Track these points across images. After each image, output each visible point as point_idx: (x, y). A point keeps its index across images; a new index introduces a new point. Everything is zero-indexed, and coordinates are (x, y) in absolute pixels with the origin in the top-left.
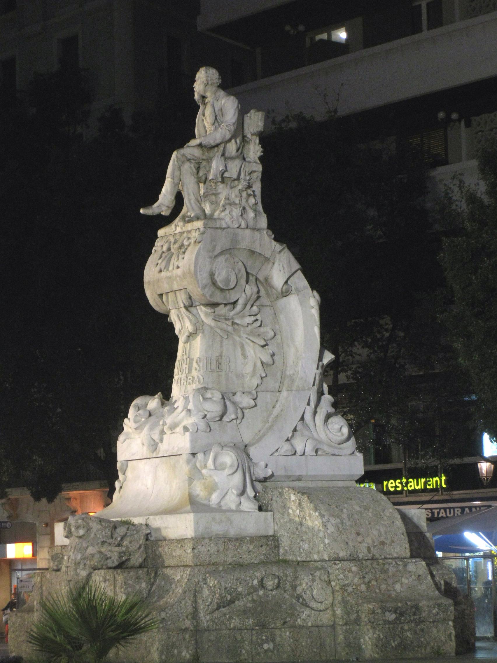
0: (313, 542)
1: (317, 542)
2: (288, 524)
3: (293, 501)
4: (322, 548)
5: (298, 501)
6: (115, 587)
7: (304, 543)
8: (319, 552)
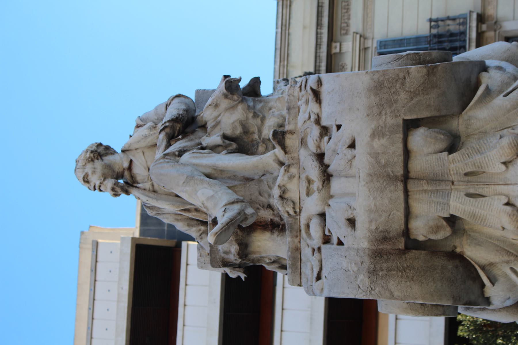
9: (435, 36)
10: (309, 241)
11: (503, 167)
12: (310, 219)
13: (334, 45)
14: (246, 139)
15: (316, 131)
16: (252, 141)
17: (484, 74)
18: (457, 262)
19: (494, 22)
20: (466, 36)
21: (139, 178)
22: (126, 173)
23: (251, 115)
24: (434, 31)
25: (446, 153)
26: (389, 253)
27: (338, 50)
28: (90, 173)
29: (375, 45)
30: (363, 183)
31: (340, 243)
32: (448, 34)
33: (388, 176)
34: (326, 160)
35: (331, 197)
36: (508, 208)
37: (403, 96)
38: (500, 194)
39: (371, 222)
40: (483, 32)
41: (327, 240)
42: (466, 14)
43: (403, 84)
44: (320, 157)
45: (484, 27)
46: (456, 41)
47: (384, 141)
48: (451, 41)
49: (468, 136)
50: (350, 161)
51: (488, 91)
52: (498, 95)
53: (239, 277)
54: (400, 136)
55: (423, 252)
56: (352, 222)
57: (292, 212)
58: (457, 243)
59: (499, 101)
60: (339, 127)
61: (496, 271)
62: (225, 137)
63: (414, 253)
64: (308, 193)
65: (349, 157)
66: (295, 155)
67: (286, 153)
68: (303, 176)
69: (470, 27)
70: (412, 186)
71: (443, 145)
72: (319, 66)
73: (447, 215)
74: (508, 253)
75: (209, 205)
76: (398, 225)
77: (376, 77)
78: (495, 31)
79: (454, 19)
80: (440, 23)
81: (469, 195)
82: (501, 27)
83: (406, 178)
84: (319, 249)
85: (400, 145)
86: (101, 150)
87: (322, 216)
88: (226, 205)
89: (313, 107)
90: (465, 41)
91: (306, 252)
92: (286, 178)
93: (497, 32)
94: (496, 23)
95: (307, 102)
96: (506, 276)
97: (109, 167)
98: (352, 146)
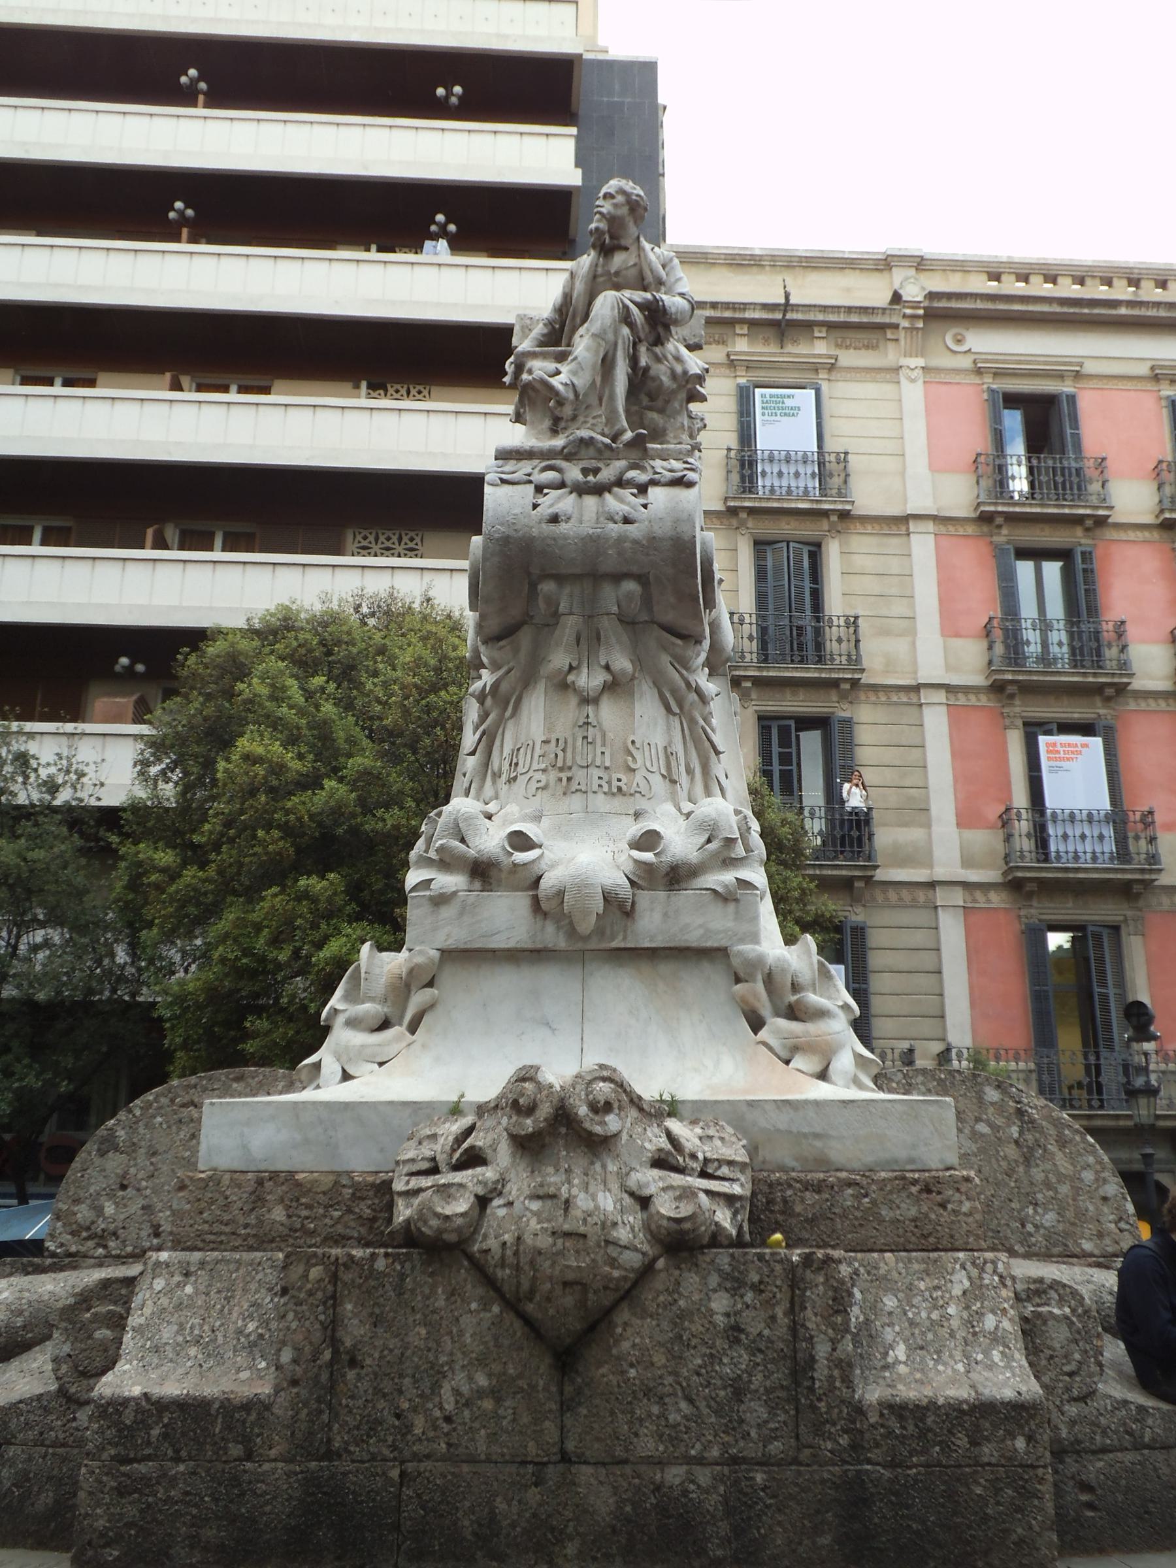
1: (1091, 1208)
3: (992, 1104)
6: (795, 1307)
11: (603, 663)
13: (824, 329)
27: (817, 334)
30: (591, 531)
31: (535, 506)
35: (580, 495)
36: (567, 667)
39: (554, 539)
40: (828, 517)
44: (620, 483)
45: (834, 518)
52: (672, 656)
53: (506, 374)
54: (635, 569)
60: (645, 506)
62: (647, 369)
64: (585, 472)
65: (616, 518)
68: (600, 465)
72: (797, 311)
79: (845, 482)
80: (842, 465)
84: (530, 482)
87: (562, 485)
88: (573, 385)
91: (525, 467)
95: (671, 471)
98: (627, 520)
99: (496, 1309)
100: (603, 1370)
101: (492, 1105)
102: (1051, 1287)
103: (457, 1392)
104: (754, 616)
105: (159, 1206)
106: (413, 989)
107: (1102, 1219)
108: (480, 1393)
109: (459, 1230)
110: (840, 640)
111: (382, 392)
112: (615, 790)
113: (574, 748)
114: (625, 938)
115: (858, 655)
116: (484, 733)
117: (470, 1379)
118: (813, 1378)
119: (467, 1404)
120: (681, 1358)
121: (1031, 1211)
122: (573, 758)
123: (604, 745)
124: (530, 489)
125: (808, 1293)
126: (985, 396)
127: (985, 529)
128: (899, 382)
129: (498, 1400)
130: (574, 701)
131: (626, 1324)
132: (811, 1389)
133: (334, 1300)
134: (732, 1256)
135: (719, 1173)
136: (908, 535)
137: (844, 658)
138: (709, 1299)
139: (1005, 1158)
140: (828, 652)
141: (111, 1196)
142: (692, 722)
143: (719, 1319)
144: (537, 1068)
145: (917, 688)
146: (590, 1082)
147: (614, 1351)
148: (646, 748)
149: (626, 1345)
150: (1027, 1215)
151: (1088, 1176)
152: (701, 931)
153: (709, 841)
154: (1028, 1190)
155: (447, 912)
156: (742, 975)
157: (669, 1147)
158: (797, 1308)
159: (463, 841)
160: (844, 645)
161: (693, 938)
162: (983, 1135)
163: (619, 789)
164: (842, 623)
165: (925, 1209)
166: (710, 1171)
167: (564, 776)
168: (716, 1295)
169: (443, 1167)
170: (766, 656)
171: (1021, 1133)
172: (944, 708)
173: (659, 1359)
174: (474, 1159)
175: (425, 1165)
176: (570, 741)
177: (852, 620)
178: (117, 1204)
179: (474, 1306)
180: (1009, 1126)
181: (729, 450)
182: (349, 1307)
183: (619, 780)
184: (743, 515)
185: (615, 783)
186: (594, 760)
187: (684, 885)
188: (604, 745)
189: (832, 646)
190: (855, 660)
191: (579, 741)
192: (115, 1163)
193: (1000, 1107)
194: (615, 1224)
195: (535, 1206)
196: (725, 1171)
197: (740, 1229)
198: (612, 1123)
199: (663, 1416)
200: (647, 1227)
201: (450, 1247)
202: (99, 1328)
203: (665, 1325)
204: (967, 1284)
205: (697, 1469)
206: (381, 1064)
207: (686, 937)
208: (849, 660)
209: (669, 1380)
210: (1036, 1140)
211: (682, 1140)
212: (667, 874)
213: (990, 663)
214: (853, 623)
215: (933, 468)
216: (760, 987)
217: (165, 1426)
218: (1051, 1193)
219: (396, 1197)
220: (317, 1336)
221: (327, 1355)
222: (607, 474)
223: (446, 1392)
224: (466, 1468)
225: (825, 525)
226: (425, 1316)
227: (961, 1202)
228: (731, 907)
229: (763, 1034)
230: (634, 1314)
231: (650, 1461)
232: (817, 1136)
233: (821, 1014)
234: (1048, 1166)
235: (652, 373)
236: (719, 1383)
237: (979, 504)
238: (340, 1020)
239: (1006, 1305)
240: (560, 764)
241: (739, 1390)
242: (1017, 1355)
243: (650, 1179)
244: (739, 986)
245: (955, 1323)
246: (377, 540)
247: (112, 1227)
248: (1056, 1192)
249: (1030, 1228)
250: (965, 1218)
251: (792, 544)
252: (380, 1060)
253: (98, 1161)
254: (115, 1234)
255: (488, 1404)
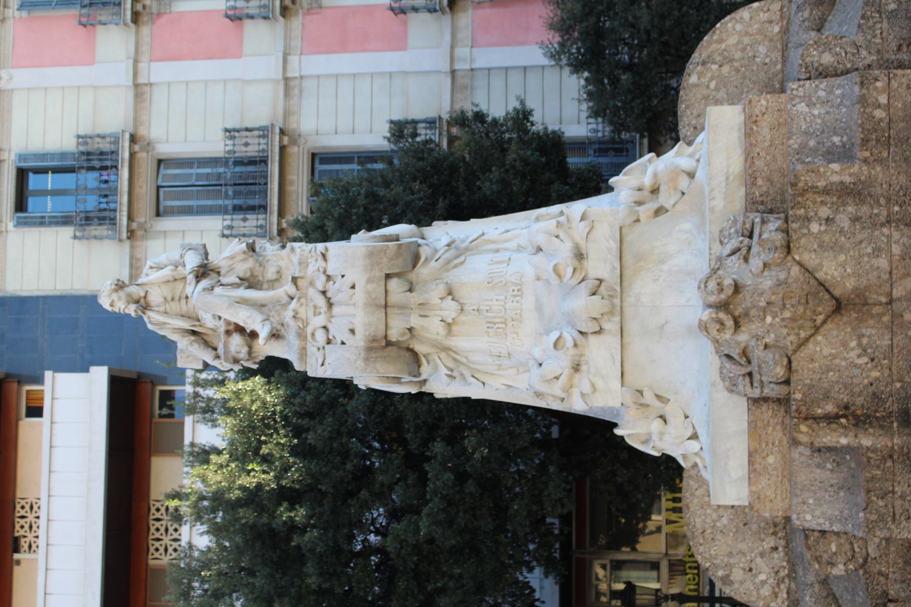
0: (756, 34)
1: (756, 26)
2: (730, 90)
3: (699, 79)
4: (766, 15)
5: (699, 68)
7: (757, 55)
8: (771, 22)
9: (83, 153)
10: (314, 343)
11: (440, 301)
12: (315, 330)
14: (252, 280)
15: (323, 278)
16: (258, 281)
17: (420, 248)
18: (410, 353)
19: (146, 143)
20: (118, 155)
21: (152, 304)
22: (142, 301)
23: (258, 265)
24: (82, 148)
25: (409, 293)
26: (376, 348)
28: (116, 299)
29: (13, 157)
31: (343, 343)
32: (98, 152)
33: (376, 305)
34: (329, 295)
35: (332, 317)
36: (442, 323)
37: (385, 260)
38: (438, 315)
39: (365, 331)
41: (329, 342)
42: (119, 133)
43: (385, 253)
45: (137, 148)
46: (107, 160)
47: (374, 285)
48: (100, 160)
49: (417, 283)
50: (351, 296)
51: (426, 259)
54: (383, 282)
55: (395, 347)
56: (352, 331)
57: (301, 326)
58: (410, 342)
59: (433, 264)
61: (430, 358)
63: (390, 348)
66: (304, 291)
67: (298, 290)
68: (311, 304)
69: (122, 146)
70: (389, 310)
71: (407, 288)
73: (409, 327)
74: (438, 348)
75: (249, 321)
76: (381, 333)
77: (369, 249)
78: (148, 152)
79: (103, 137)
80: (89, 140)
81: (421, 316)
82: (154, 149)
83: (386, 306)
84: (324, 348)
85: (383, 288)
86: (120, 283)
89: (321, 263)
90: (117, 161)
92: (298, 305)
93: (150, 154)
94: (148, 144)
96: (434, 360)
97: (129, 295)
98: (353, 287)
99: (819, 338)
100: (848, 285)
101: (717, 345)
102: (803, 60)
103: (859, 356)
104: (226, 217)
105: (761, 549)
106: (643, 401)
107: (762, 21)
108: (860, 345)
109: (781, 356)
110: (247, 144)
111: (23, 540)
112: (520, 293)
113: (495, 317)
114: (615, 284)
115: (259, 129)
116: (473, 376)
117: (853, 349)
118: (850, 183)
119: (865, 351)
120: (841, 247)
121: (758, 60)
122: (500, 318)
123: (492, 300)
124: (327, 347)
125: (810, 185)
126: (24, 14)
127: (145, 18)
128: (12, 90)
129: (863, 336)
130: (463, 318)
131: (826, 274)
132: (854, 184)
133: (816, 419)
134: (793, 222)
135: (750, 229)
136: (151, 84)
137: (262, 141)
138: (813, 233)
139: (729, 73)
140: (256, 154)
141: (756, 576)
142: (467, 249)
143: (823, 228)
144: (700, 320)
145: (286, 79)
146: (708, 294)
147: (839, 279)
148: (492, 275)
149: (836, 274)
150: (760, 62)
151: (739, 27)
152: (611, 241)
153: (557, 237)
154: (746, 61)
155: (599, 384)
156: (635, 218)
157: (737, 254)
158: (817, 190)
159: (557, 378)
160: (249, 141)
161: (614, 245)
162: (716, 85)
163: (518, 290)
164: (230, 142)
165: (765, 124)
166: (748, 234)
167: (510, 323)
168: (812, 230)
169: (748, 370)
170: (260, 207)
171: (715, 63)
172: (303, 57)
173: (842, 257)
174: (744, 353)
175: (747, 379)
176: (489, 320)
177: (228, 134)
178: (760, 573)
179: (818, 349)
180: (712, 70)
181: (75, 237)
182: (819, 411)
183: (513, 291)
184: (134, 226)
185: (516, 293)
186: (502, 306)
187: (584, 252)
188: (492, 300)
189: (252, 151)
190: (264, 132)
191: (489, 314)
192: (737, 575)
193: (701, 75)
194: (778, 280)
195: (769, 319)
196: (748, 226)
197: (779, 219)
198: (728, 282)
199: (869, 255)
200: (779, 265)
201: (790, 362)
202: (831, 549)
203: (826, 254)
204: (803, 104)
205: (893, 239)
206: (686, 417)
207: (614, 250)
208: (264, 136)
209: (852, 253)
210: (720, 54)
211: (733, 247)
212: (578, 260)
213: (265, 18)
214: (230, 133)
215: (90, 61)
216: (641, 209)
217: (878, 498)
218: (748, 48)
219: (763, 394)
220: (833, 426)
221: (843, 421)
222: (321, 302)
223: (860, 361)
224: (895, 351)
225: (142, 155)
226: (823, 373)
227: (762, 105)
228: (596, 224)
229: (668, 206)
230: (821, 270)
231: (891, 262)
232: (727, 179)
233: (655, 175)
234: (733, 49)
235: (242, 275)
236: (852, 228)
237: (125, 24)
238: (659, 444)
239: (813, 85)
240: (503, 326)
241: (855, 219)
242: (838, 82)
243: (756, 263)
244: (642, 220)
245: (823, 111)
246: (158, 540)
247: (773, 575)
248: (748, 45)
249: (767, 60)
250: (770, 103)
251: (160, 183)
252: (683, 418)
253: (736, 586)
254: (777, 573)
255: (865, 341)
